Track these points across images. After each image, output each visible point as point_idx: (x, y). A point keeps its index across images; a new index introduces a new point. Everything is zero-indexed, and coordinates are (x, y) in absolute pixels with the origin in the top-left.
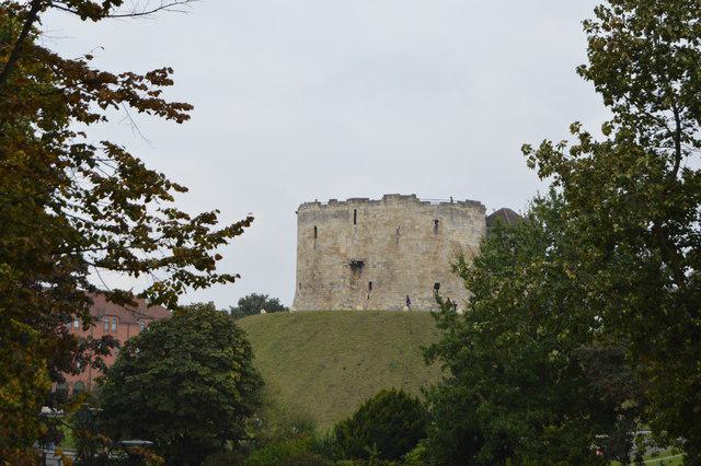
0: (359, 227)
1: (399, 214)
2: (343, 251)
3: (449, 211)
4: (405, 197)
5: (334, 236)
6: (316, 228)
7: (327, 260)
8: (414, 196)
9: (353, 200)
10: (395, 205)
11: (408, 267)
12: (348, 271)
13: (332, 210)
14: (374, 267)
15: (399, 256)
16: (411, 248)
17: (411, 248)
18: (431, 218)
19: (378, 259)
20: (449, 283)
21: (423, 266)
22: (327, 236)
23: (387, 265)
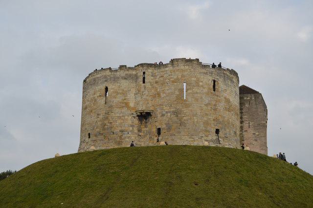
0: (147, 85)
1: (185, 73)
2: (132, 105)
3: (223, 75)
4: (190, 61)
5: (124, 93)
6: (107, 89)
7: (117, 112)
8: (198, 60)
9: (142, 65)
10: (182, 66)
11: (196, 115)
12: (136, 121)
13: (122, 73)
14: (163, 115)
15: (187, 106)
16: (197, 100)
17: (197, 100)
18: (211, 78)
19: (166, 109)
20: (225, 130)
21: (207, 114)
22: (118, 93)
23: (176, 113)
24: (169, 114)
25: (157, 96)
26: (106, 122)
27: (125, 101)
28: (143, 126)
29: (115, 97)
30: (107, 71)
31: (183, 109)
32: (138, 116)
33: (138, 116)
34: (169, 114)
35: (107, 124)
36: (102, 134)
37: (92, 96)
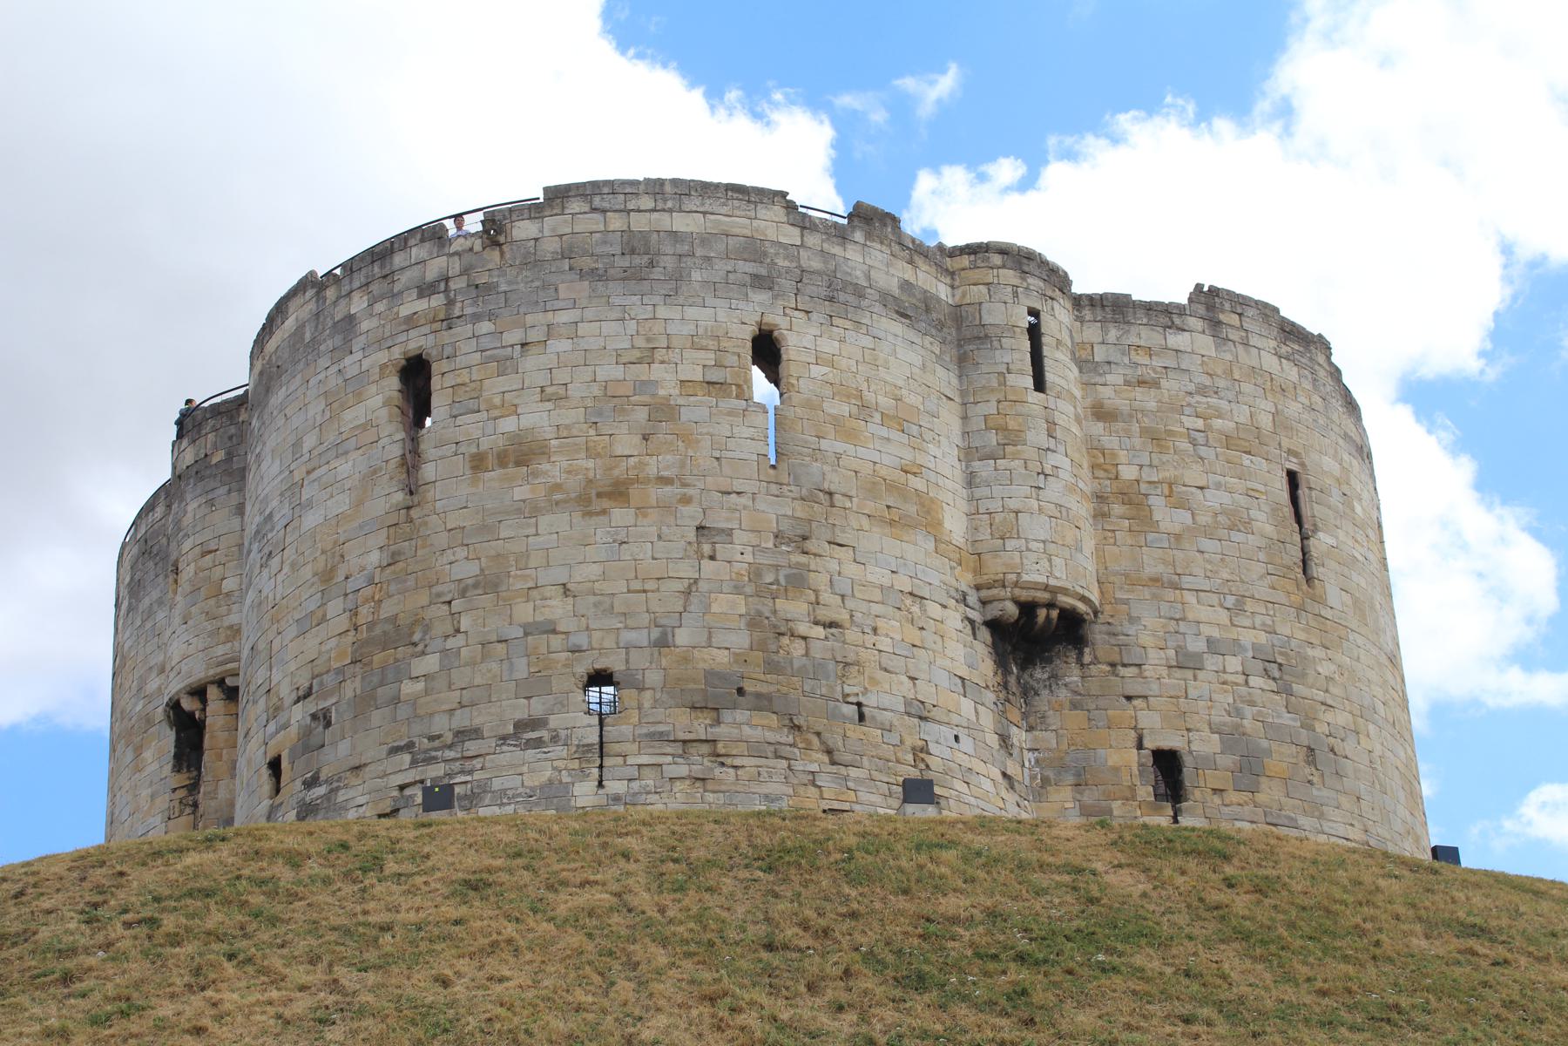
1: (1293, 409)
2: (955, 524)
10: (1266, 353)
14: (1187, 663)
19: (1209, 617)
24: (1234, 664)
25: (1118, 509)
26: (794, 609)
27: (917, 483)
28: (1015, 715)
29: (851, 436)
30: (762, 212)
31: (1310, 652)
32: (994, 625)
33: (994, 625)
34: (1234, 664)
35: (803, 628)
36: (763, 703)
37: (610, 371)
